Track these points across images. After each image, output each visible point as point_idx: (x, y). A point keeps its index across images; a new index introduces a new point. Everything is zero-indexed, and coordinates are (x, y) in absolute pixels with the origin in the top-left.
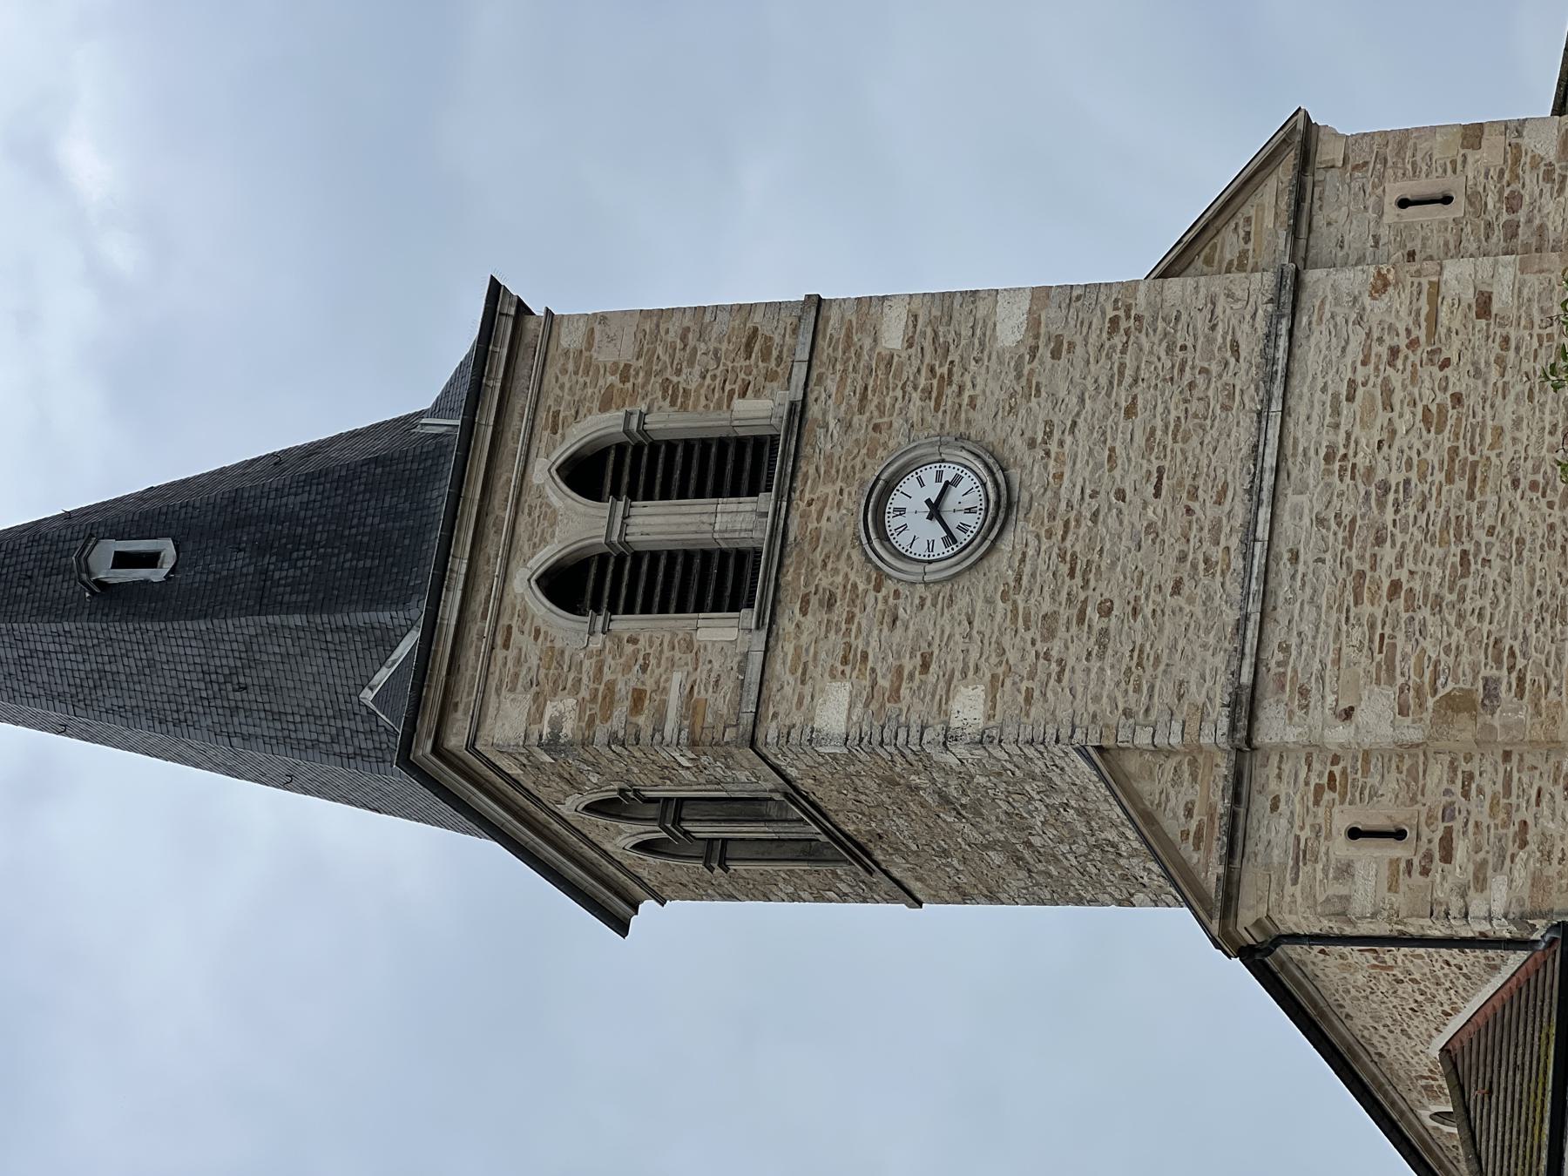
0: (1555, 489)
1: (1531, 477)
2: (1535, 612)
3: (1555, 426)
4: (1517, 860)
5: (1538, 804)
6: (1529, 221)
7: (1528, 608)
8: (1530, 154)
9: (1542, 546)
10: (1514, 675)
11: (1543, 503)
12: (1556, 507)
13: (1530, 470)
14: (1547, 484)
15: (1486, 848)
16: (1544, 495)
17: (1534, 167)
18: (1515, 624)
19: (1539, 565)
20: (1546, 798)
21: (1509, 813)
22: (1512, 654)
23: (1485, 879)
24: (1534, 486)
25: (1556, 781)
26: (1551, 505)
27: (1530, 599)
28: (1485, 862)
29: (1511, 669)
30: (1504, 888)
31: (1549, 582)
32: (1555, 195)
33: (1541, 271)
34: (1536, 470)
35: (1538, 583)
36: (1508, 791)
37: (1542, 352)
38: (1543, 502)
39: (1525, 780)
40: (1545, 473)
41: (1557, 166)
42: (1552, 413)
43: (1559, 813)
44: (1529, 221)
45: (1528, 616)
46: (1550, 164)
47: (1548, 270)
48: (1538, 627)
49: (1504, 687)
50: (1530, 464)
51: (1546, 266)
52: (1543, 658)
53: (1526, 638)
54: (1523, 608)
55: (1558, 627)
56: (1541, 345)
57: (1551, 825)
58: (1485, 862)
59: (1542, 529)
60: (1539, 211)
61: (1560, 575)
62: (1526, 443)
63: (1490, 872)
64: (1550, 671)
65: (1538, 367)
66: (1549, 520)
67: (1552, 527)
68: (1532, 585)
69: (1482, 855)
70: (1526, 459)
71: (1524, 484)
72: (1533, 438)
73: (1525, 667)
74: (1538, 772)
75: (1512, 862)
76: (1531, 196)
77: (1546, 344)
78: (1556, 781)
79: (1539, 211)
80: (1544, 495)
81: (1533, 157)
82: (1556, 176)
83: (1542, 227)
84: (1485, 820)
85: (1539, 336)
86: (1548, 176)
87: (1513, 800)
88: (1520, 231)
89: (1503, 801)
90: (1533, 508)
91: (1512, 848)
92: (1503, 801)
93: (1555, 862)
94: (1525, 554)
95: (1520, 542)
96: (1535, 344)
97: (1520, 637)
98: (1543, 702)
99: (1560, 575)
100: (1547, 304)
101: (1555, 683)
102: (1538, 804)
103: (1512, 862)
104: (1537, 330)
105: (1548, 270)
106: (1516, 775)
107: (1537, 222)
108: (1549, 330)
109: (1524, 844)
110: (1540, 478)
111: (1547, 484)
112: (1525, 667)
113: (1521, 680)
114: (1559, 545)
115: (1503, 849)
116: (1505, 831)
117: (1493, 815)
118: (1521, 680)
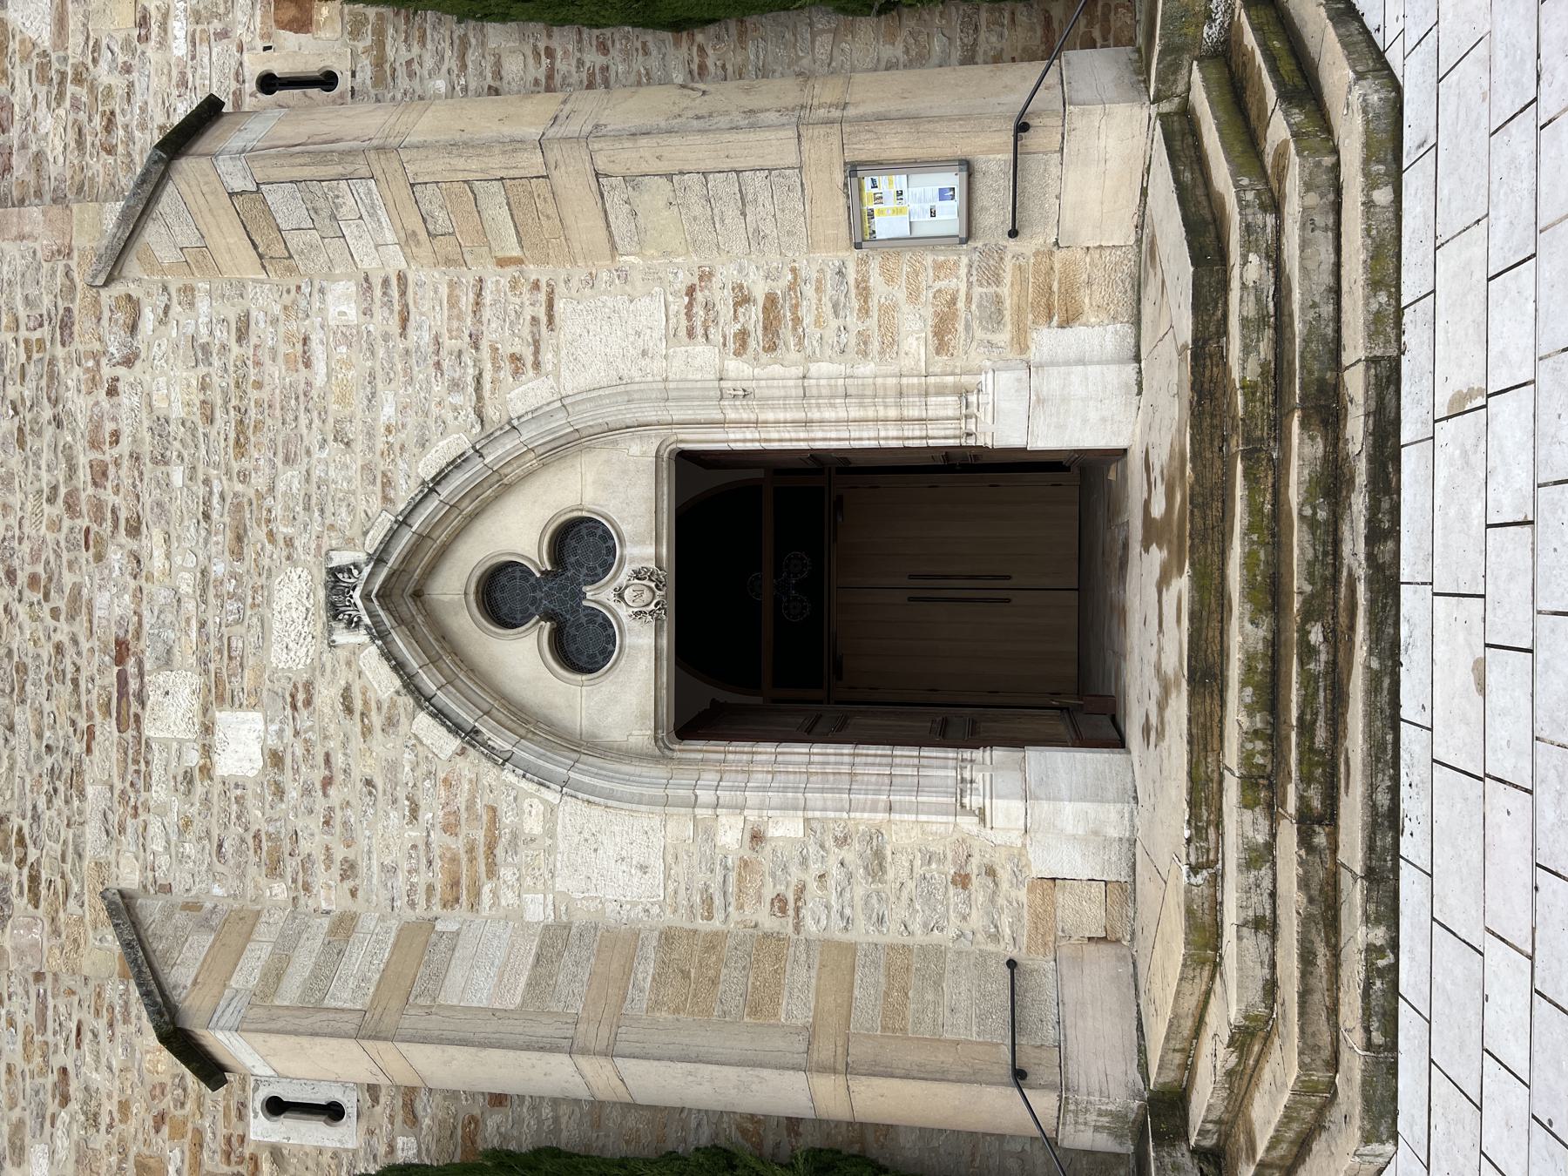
0: (61, 590)
1: (29, 569)
2: (45, 779)
3: (55, 488)
4: (58, 1123)
5: (78, 1046)
6: (24, 146)
7: (36, 771)
8: (18, 38)
9: (48, 678)
10: (26, 871)
11: (45, 613)
12: (62, 618)
13: (27, 558)
14: (50, 579)
15: (22, 1103)
16: (46, 597)
17: (25, 58)
18: (23, 795)
19: (47, 707)
20: (87, 1037)
21: (44, 1056)
22: (21, 841)
23: (22, 1148)
24: (34, 580)
25: (98, 1013)
26: (55, 613)
27: (38, 758)
28: (21, 1122)
29: (21, 862)
30: (44, 1162)
31: (61, 733)
32: (54, 105)
33: (22, 237)
34: (35, 558)
35: (47, 734)
36: (42, 1026)
37: (31, 370)
38: (47, 607)
39: (62, 1009)
40: (47, 563)
41: (54, 57)
42: (49, 469)
43: (104, 1061)
44: (24, 146)
45: (37, 783)
46: (45, 54)
47: (30, 236)
48: (50, 801)
49: (15, 889)
50: (26, 546)
51: (27, 229)
52: (58, 848)
53: (36, 817)
54: (30, 770)
55: (76, 803)
56: (29, 358)
57: (95, 1075)
58: (21, 1122)
59: (47, 650)
60: (34, 131)
61: (73, 723)
62: (20, 514)
63: (28, 1140)
64: (67, 867)
65: (26, 393)
66: (56, 637)
67: (59, 648)
68: (39, 736)
69: (17, 1112)
70: (20, 541)
71: (22, 578)
72: (29, 506)
73: (38, 861)
74: (76, 999)
75: (53, 1126)
76: (22, 106)
77: (35, 356)
78: (98, 1013)
79: (34, 131)
80: (46, 597)
81: (22, 42)
82: (53, 73)
83: (39, 156)
84: (19, 1063)
85: (26, 341)
86: (43, 68)
87: (49, 1037)
88: (15, 160)
89: (38, 1038)
90: (35, 618)
91: (52, 1106)
92: (38, 1038)
93: (103, 1128)
94: (29, 688)
95: (22, 669)
96: (23, 358)
97: (29, 814)
98: (62, 915)
99: (73, 723)
100: (33, 291)
101: (76, 888)
102: (78, 1046)
103: (53, 1126)
104: (23, 333)
105: (30, 236)
106: (51, 1002)
107: (34, 148)
108: (37, 334)
109: (65, 1100)
110: (40, 569)
111: (50, 579)
112: (38, 861)
113: (34, 879)
114: (69, 676)
115: (42, 1105)
116: (41, 1080)
117: (28, 1058)
118: (34, 879)
